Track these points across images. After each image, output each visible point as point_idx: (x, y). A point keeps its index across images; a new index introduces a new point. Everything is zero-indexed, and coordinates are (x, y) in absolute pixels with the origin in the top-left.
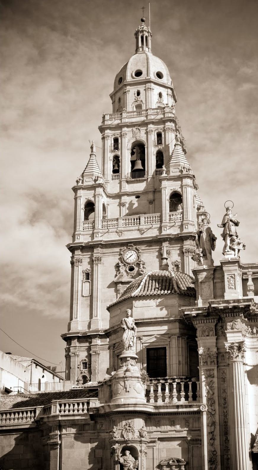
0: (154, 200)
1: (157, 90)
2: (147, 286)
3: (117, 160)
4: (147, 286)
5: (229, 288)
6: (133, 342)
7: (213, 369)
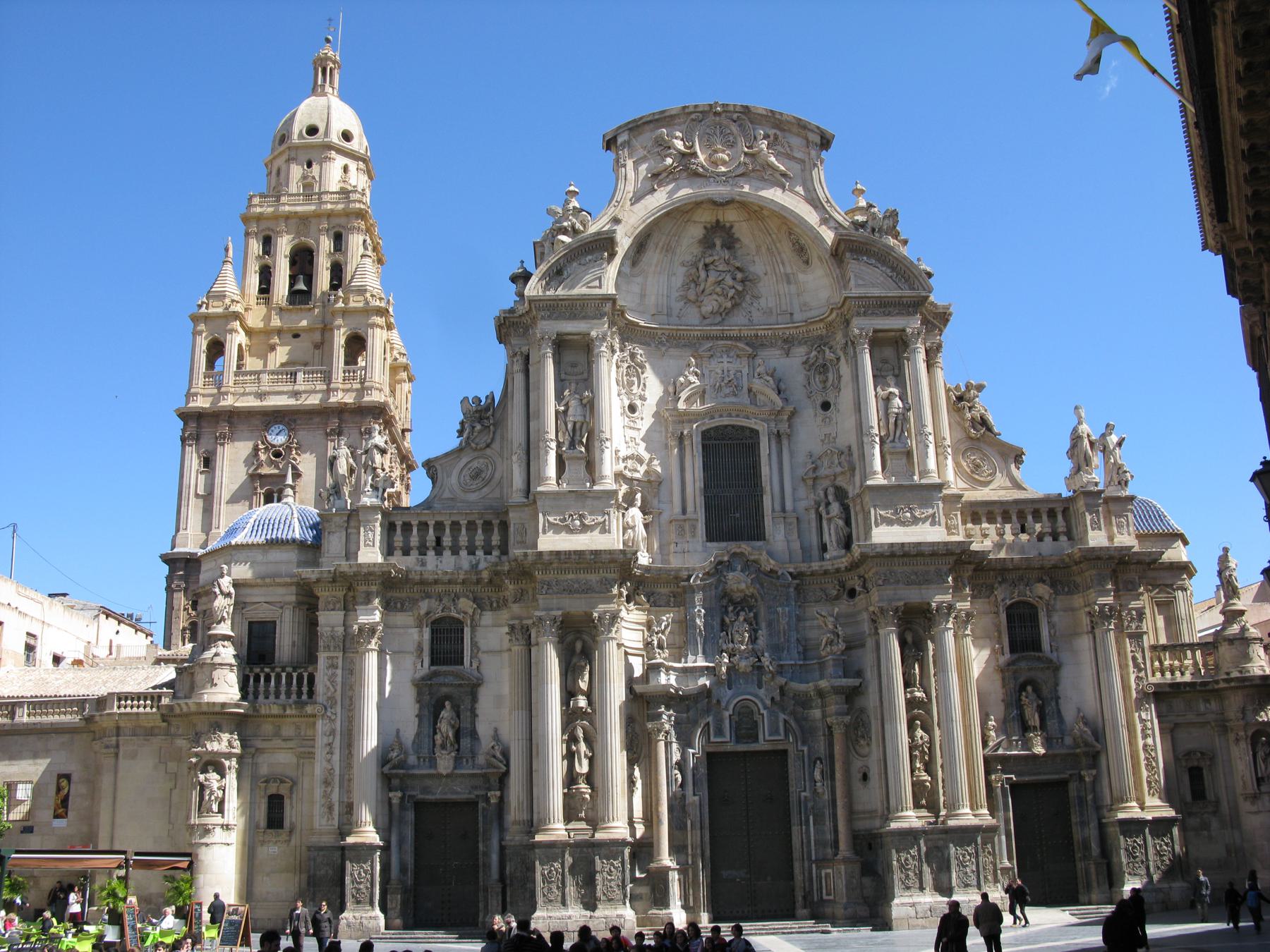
0: (322, 343)
1: (340, 161)
2: (256, 528)
3: (266, 275)
4: (256, 528)
5: (366, 545)
6: (228, 613)
7: (337, 658)
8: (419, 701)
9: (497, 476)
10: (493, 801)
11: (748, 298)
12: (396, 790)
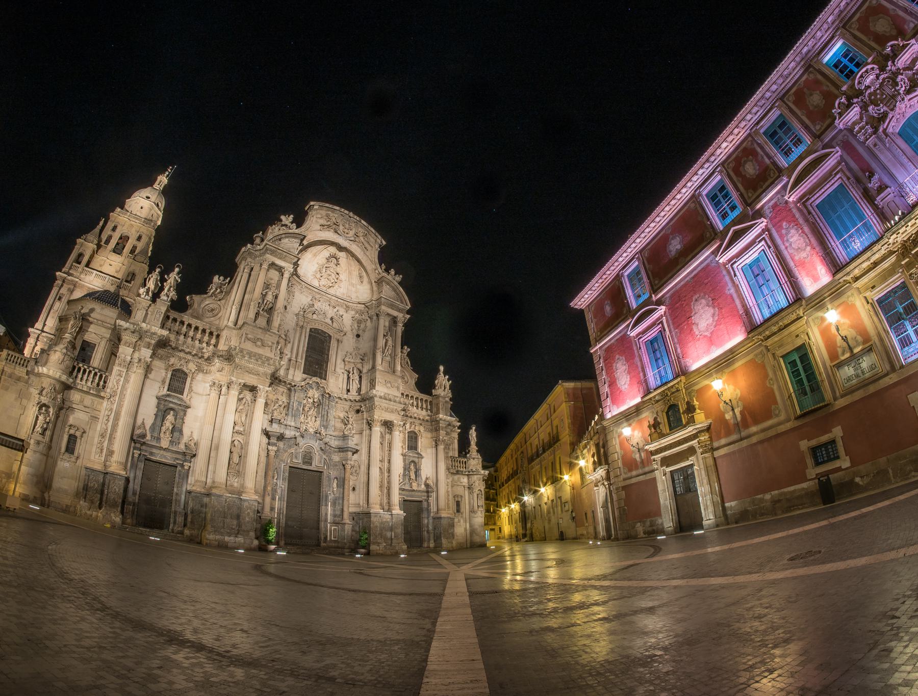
8: (158, 407)
9: (220, 315)
10: (186, 468)
11: (337, 286)
12: (137, 450)
